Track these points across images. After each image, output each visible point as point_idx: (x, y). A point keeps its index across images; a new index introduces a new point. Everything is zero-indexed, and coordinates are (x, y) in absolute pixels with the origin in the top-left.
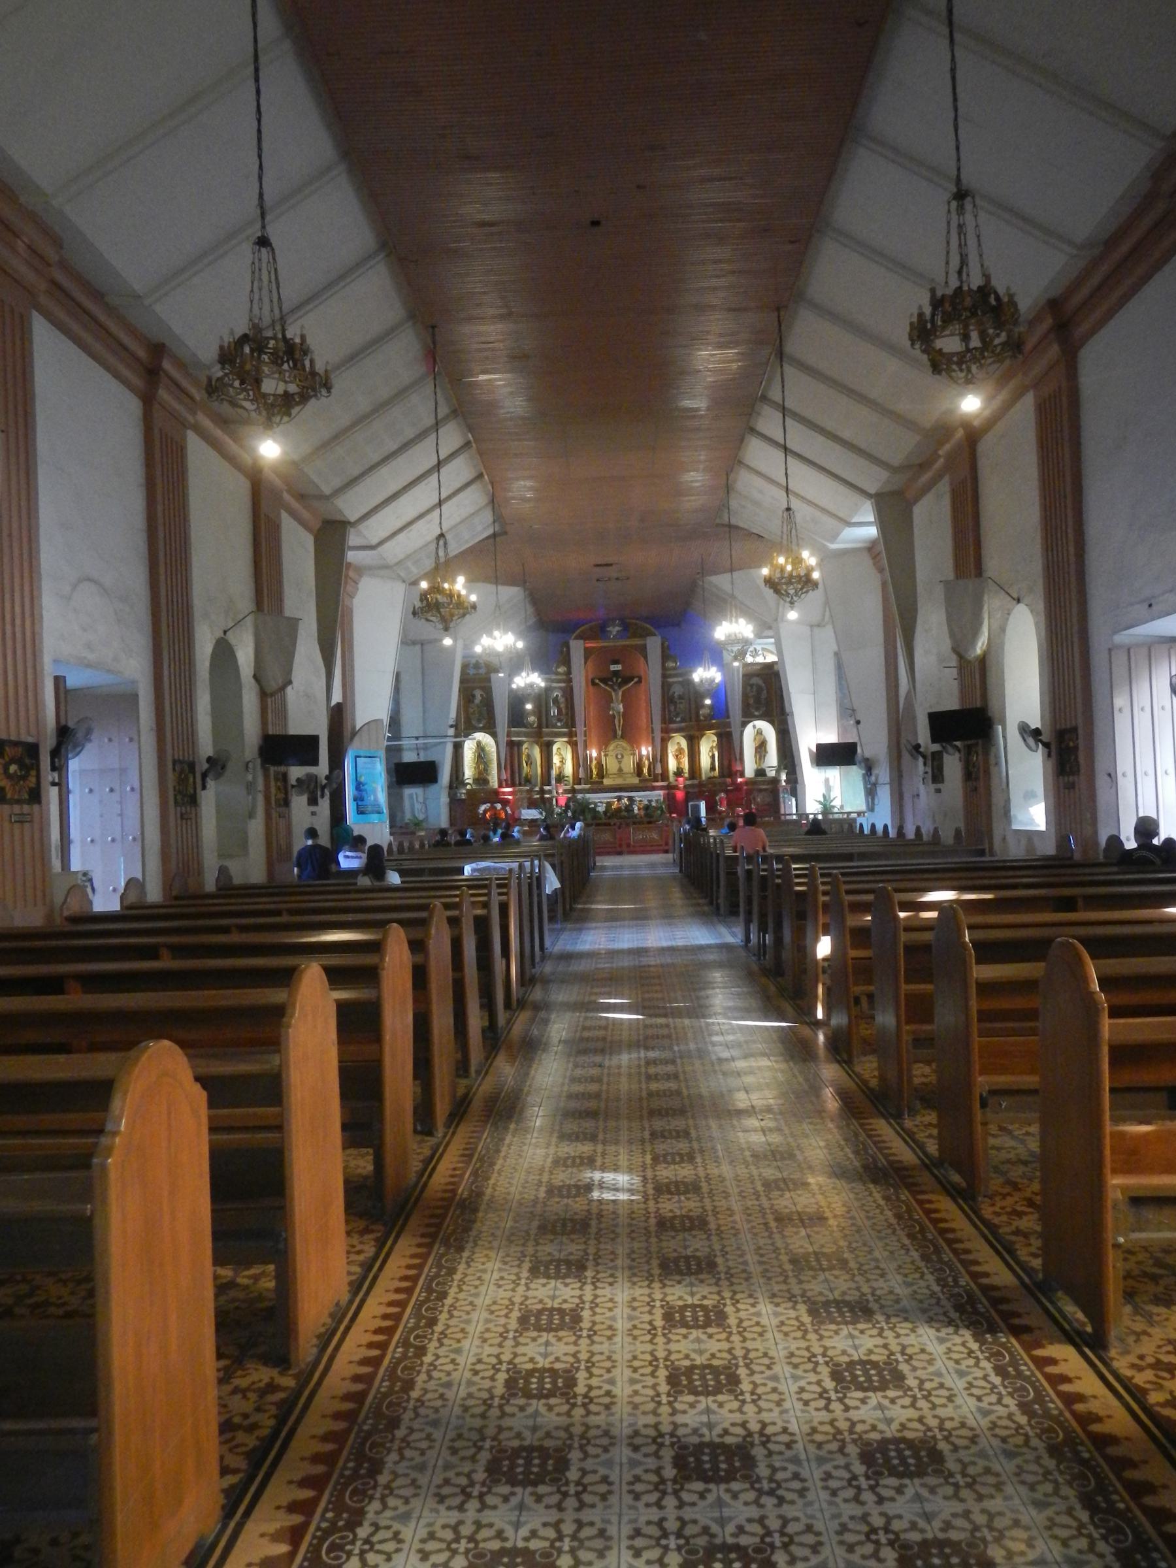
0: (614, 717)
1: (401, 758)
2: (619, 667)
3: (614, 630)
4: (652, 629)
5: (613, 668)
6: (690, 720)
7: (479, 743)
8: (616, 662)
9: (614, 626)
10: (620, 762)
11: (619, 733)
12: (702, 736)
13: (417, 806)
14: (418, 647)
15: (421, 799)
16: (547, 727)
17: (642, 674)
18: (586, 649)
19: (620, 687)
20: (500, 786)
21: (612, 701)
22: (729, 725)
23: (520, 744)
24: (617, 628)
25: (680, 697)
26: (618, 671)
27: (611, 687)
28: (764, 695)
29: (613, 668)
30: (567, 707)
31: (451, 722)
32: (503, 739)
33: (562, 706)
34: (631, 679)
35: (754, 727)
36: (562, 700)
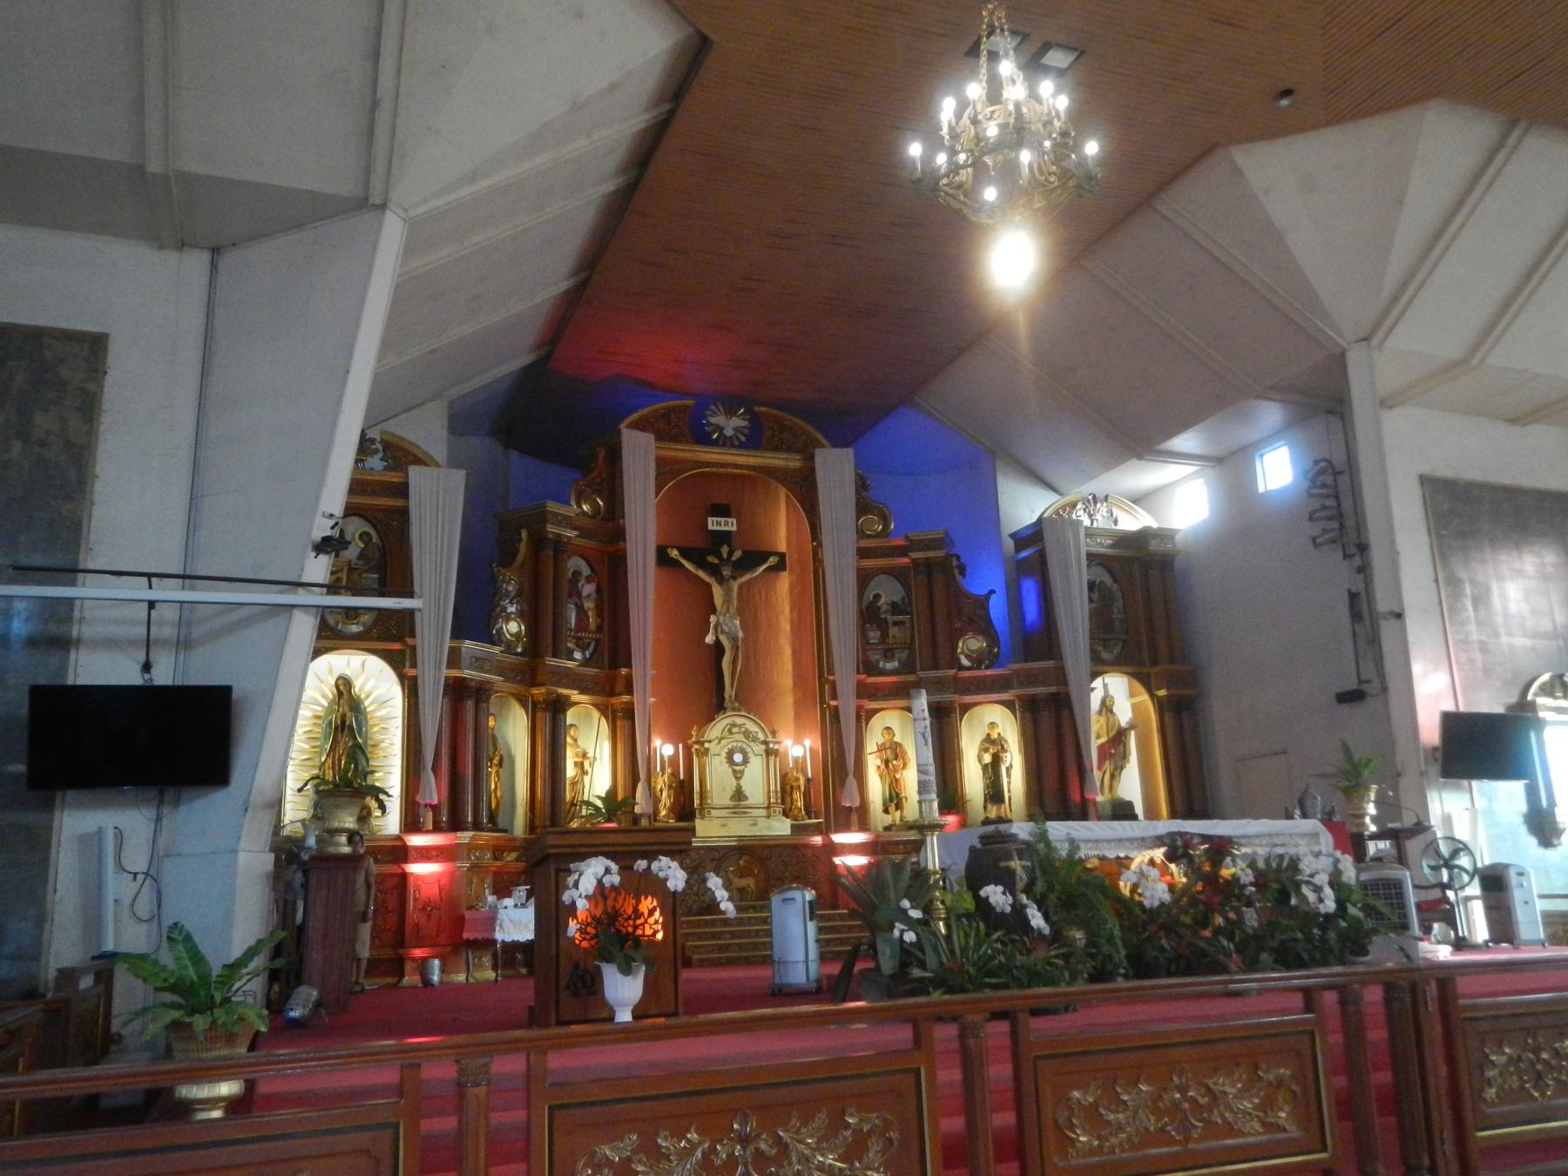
0: (718, 647)
1: (63, 668)
2: (730, 525)
3: (732, 424)
4: (824, 441)
5: (714, 524)
6: (936, 667)
7: (344, 687)
8: (722, 511)
9: (730, 412)
10: (738, 775)
11: (729, 692)
12: (966, 708)
13: (117, 887)
14: (197, 261)
15: (137, 860)
16: (554, 656)
17: (782, 547)
18: (661, 462)
19: (734, 578)
20: (412, 823)
21: (714, 611)
22: (1061, 676)
23: (481, 693)
24: (736, 422)
25: (895, 608)
26: (729, 532)
27: (714, 571)
28: (1117, 613)
29: (714, 524)
30: (599, 611)
31: (322, 529)
32: (433, 674)
33: (589, 605)
34: (763, 557)
35: (1105, 686)
36: (588, 589)
